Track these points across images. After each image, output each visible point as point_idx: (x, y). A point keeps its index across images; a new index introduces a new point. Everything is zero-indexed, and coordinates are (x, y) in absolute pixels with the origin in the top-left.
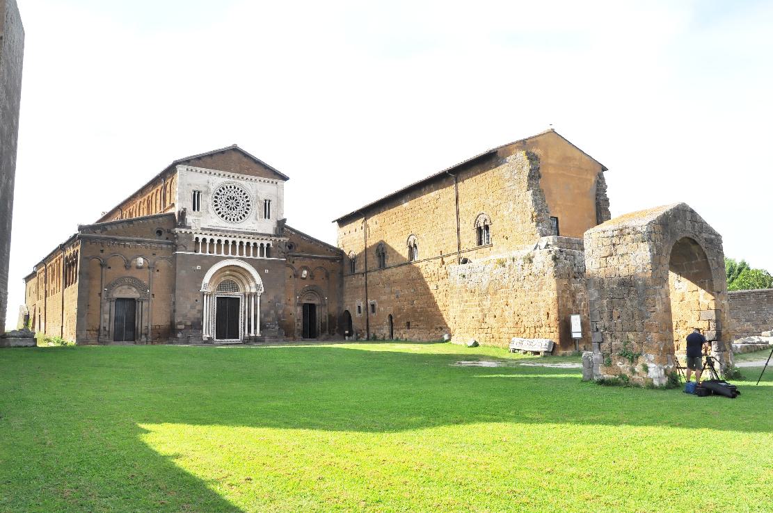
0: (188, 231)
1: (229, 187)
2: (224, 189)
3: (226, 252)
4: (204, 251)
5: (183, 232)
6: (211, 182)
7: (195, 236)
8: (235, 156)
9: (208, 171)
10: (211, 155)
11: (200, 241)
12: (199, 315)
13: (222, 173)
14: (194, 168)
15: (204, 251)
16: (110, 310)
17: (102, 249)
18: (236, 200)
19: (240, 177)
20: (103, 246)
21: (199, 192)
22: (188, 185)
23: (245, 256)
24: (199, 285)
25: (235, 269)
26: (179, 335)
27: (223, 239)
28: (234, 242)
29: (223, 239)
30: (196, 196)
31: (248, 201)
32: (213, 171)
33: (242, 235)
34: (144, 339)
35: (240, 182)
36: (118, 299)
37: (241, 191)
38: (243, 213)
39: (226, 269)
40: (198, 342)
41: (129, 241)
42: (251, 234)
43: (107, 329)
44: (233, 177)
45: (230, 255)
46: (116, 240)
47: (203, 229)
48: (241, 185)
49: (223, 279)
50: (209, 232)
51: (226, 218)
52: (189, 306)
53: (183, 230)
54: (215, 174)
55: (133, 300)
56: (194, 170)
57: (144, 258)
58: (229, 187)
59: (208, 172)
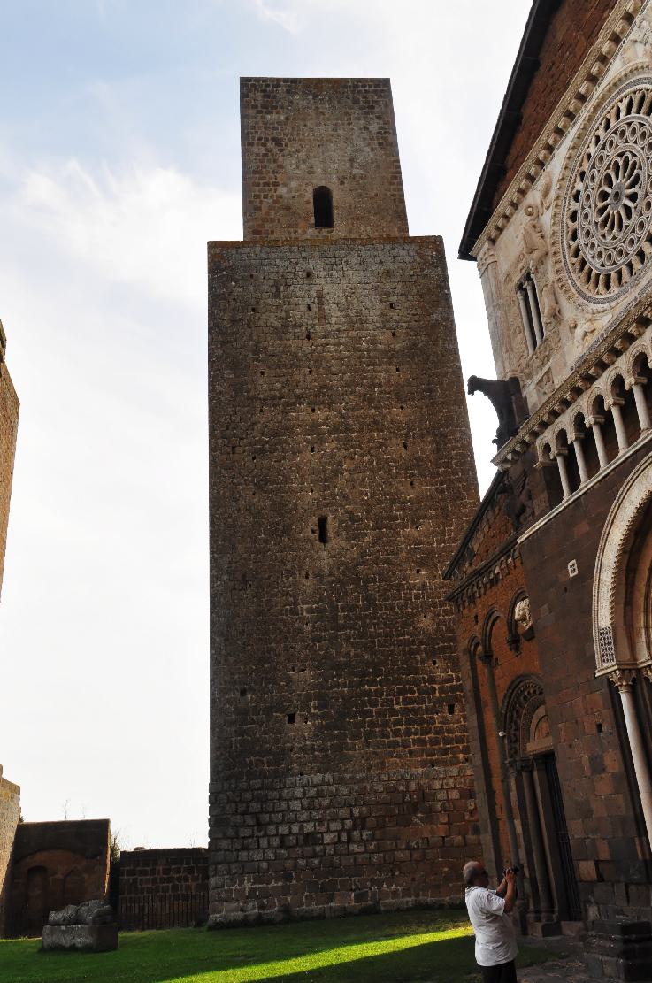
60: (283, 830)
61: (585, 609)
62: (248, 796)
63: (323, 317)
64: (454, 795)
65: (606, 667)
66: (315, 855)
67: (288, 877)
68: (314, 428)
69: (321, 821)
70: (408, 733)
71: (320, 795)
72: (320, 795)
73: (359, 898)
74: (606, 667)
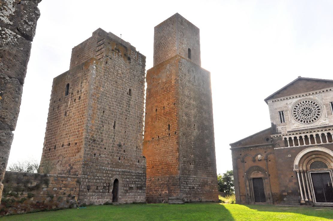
0: (278, 135)
1: (302, 102)
2: (299, 105)
3: (307, 143)
4: (291, 145)
5: (276, 136)
6: (288, 103)
7: (284, 137)
8: (301, 84)
9: (285, 98)
10: (285, 89)
11: (288, 139)
12: (296, 186)
13: (294, 96)
14: (276, 99)
15: (291, 145)
16: (249, 184)
17: (241, 153)
18: (307, 108)
19: (308, 94)
20: (241, 152)
21: (282, 112)
22: (275, 109)
23: (322, 143)
24: (291, 166)
25: (315, 153)
26: (285, 199)
27: (303, 135)
28: (312, 136)
29: (303, 135)
30: (281, 114)
31: (318, 107)
32: (288, 97)
33: (316, 130)
34: (268, 201)
35: (308, 97)
36: (254, 179)
37: (312, 102)
38: (316, 115)
39: (310, 154)
40: (297, 204)
41: (251, 147)
42: (325, 127)
43: (249, 195)
44: (303, 96)
45: (310, 144)
46: (246, 148)
47: (288, 132)
48: (310, 99)
49: (313, 161)
50: (292, 133)
51: (304, 122)
52: (288, 181)
53: (275, 136)
54: (293, 97)
55: (261, 178)
56: (277, 100)
57: (261, 155)
58: (302, 102)
59: (285, 99)
60: (190, 185)
61: (293, 162)
62: (185, 178)
63: (195, 81)
64: (210, 182)
65: (294, 169)
66: (194, 191)
67: (190, 195)
68: (193, 105)
69: (194, 185)
70: (205, 170)
71: (194, 180)
72: (194, 180)
73: (199, 199)
74: (294, 169)
